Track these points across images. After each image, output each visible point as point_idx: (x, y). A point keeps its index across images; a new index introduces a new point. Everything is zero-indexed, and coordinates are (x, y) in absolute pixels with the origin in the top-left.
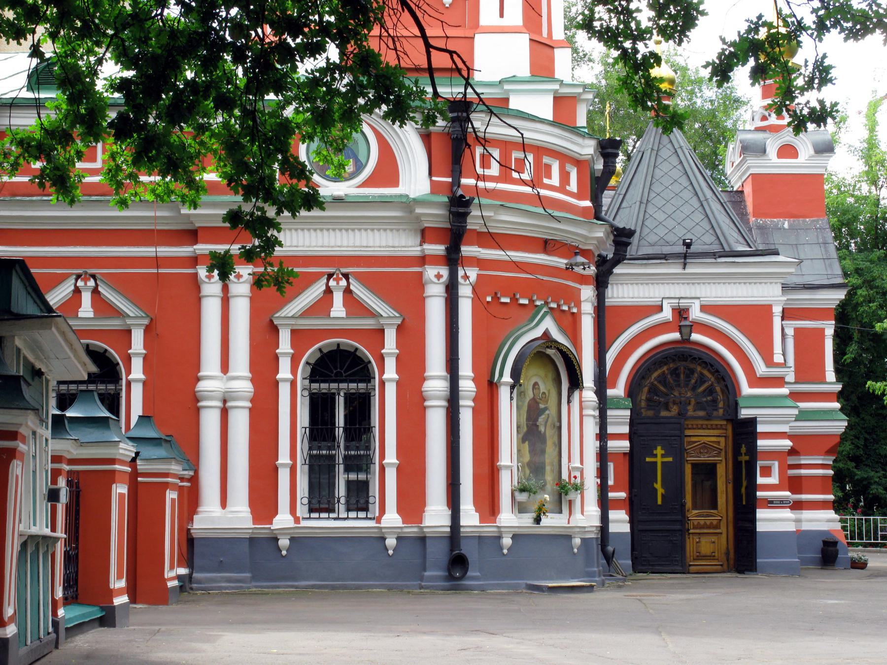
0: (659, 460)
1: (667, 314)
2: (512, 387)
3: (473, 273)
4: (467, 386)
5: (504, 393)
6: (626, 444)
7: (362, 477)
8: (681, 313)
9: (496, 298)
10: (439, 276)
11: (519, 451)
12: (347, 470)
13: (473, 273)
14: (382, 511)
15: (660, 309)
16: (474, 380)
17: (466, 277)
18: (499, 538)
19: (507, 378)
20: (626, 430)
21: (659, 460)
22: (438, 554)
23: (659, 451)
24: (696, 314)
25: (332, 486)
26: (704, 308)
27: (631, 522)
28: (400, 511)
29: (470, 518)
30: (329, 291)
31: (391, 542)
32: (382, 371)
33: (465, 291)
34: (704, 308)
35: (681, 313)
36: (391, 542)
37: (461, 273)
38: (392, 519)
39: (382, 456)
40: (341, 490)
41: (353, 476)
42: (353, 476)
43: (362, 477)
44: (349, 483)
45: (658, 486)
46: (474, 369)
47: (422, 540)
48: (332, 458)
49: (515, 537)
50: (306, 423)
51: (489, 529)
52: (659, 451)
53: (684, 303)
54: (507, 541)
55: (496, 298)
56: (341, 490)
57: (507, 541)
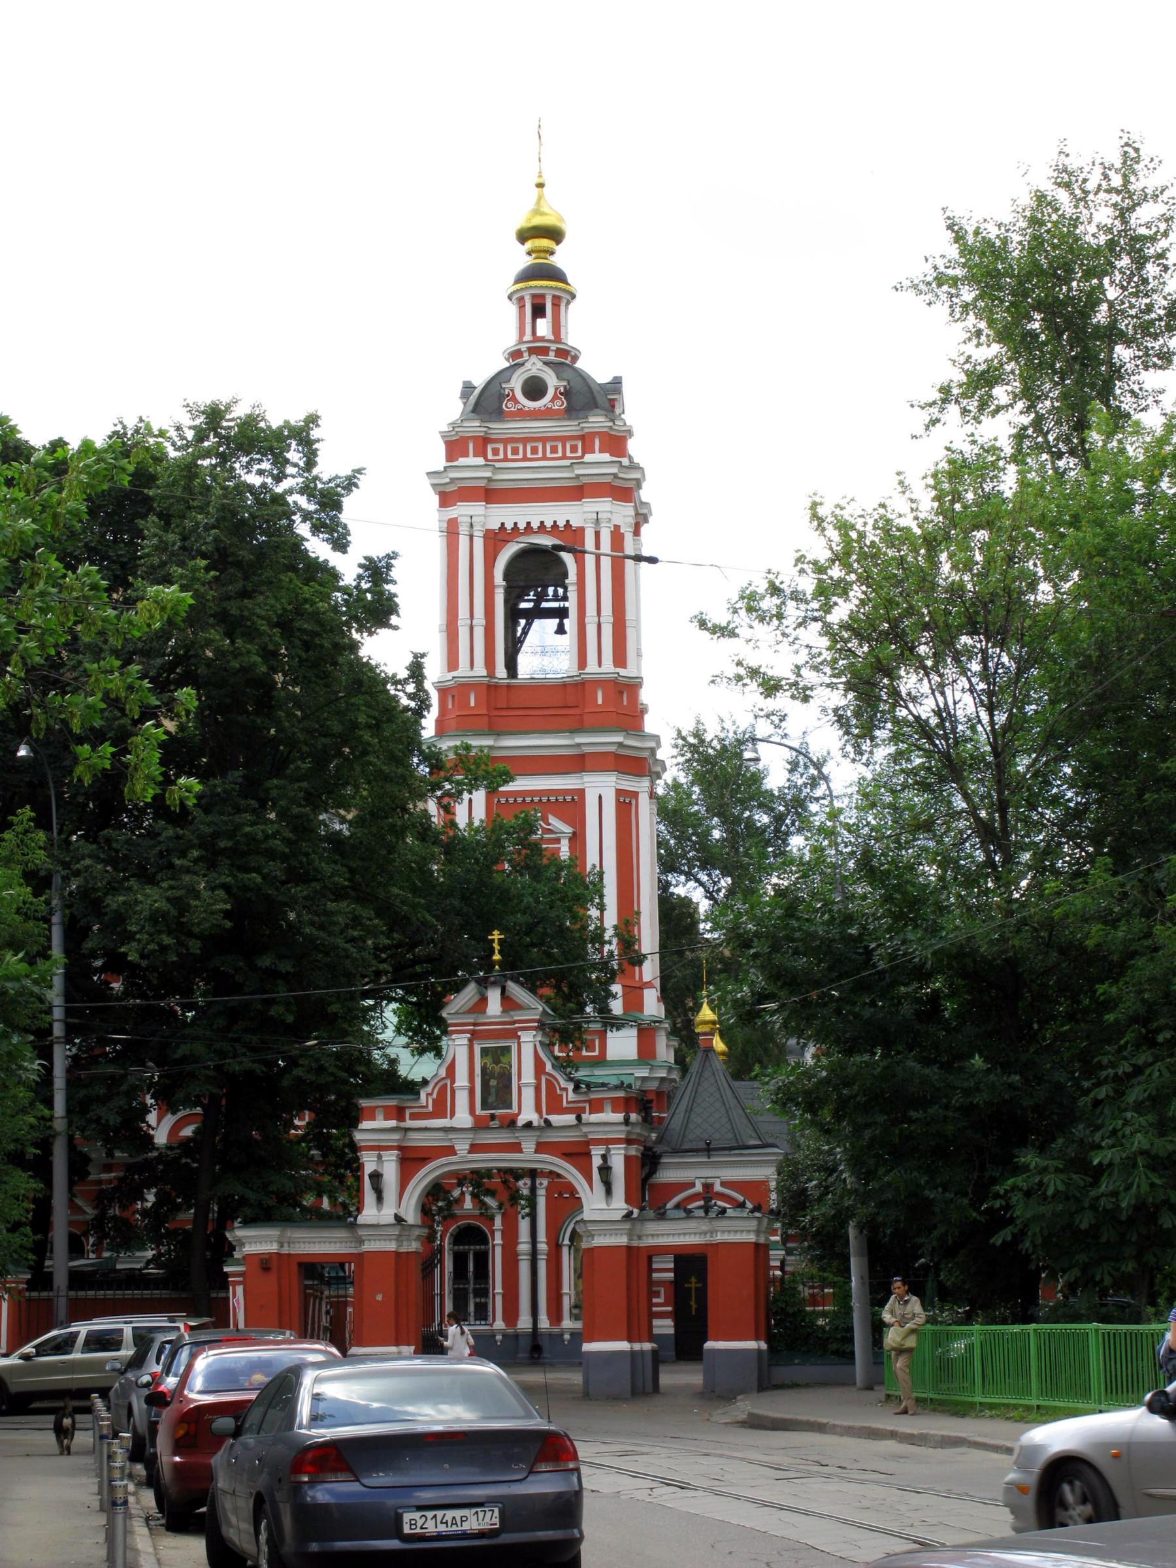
0: (693, 1285)
1: (699, 1188)
2: (570, 1247)
3: (545, 1182)
4: (543, 1247)
5: (565, 1251)
6: (672, 1275)
7: (483, 1300)
8: (708, 1187)
9: (561, 1194)
10: (525, 1184)
11: (575, 1284)
12: (475, 1296)
13: (545, 1182)
14: (494, 1320)
15: (693, 1185)
16: (547, 1243)
17: (541, 1184)
18: (562, 1335)
19: (567, 1242)
20: (672, 1266)
21: (693, 1285)
22: (525, 1344)
23: (693, 1280)
24: (718, 1188)
25: (466, 1305)
26: (723, 1184)
27: (676, 1327)
28: (505, 1319)
29: (544, 1323)
30: (463, 1193)
31: (499, 1337)
32: (493, 1239)
33: (541, 1192)
34: (723, 1184)
35: (708, 1187)
36: (499, 1337)
37: (538, 1182)
38: (499, 1324)
39: (494, 1289)
40: (471, 1308)
41: (478, 1300)
42: (478, 1300)
43: (483, 1300)
44: (477, 1305)
45: (693, 1303)
46: (547, 1237)
47: (516, 1336)
48: (466, 1290)
49: (572, 1334)
50: (451, 1270)
51: (556, 1330)
52: (693, 1280)
53: (709, 1181)
54: (567, 1337)
55: (561, 1194)
56: (471, 1308)
57: (567, 1337)
